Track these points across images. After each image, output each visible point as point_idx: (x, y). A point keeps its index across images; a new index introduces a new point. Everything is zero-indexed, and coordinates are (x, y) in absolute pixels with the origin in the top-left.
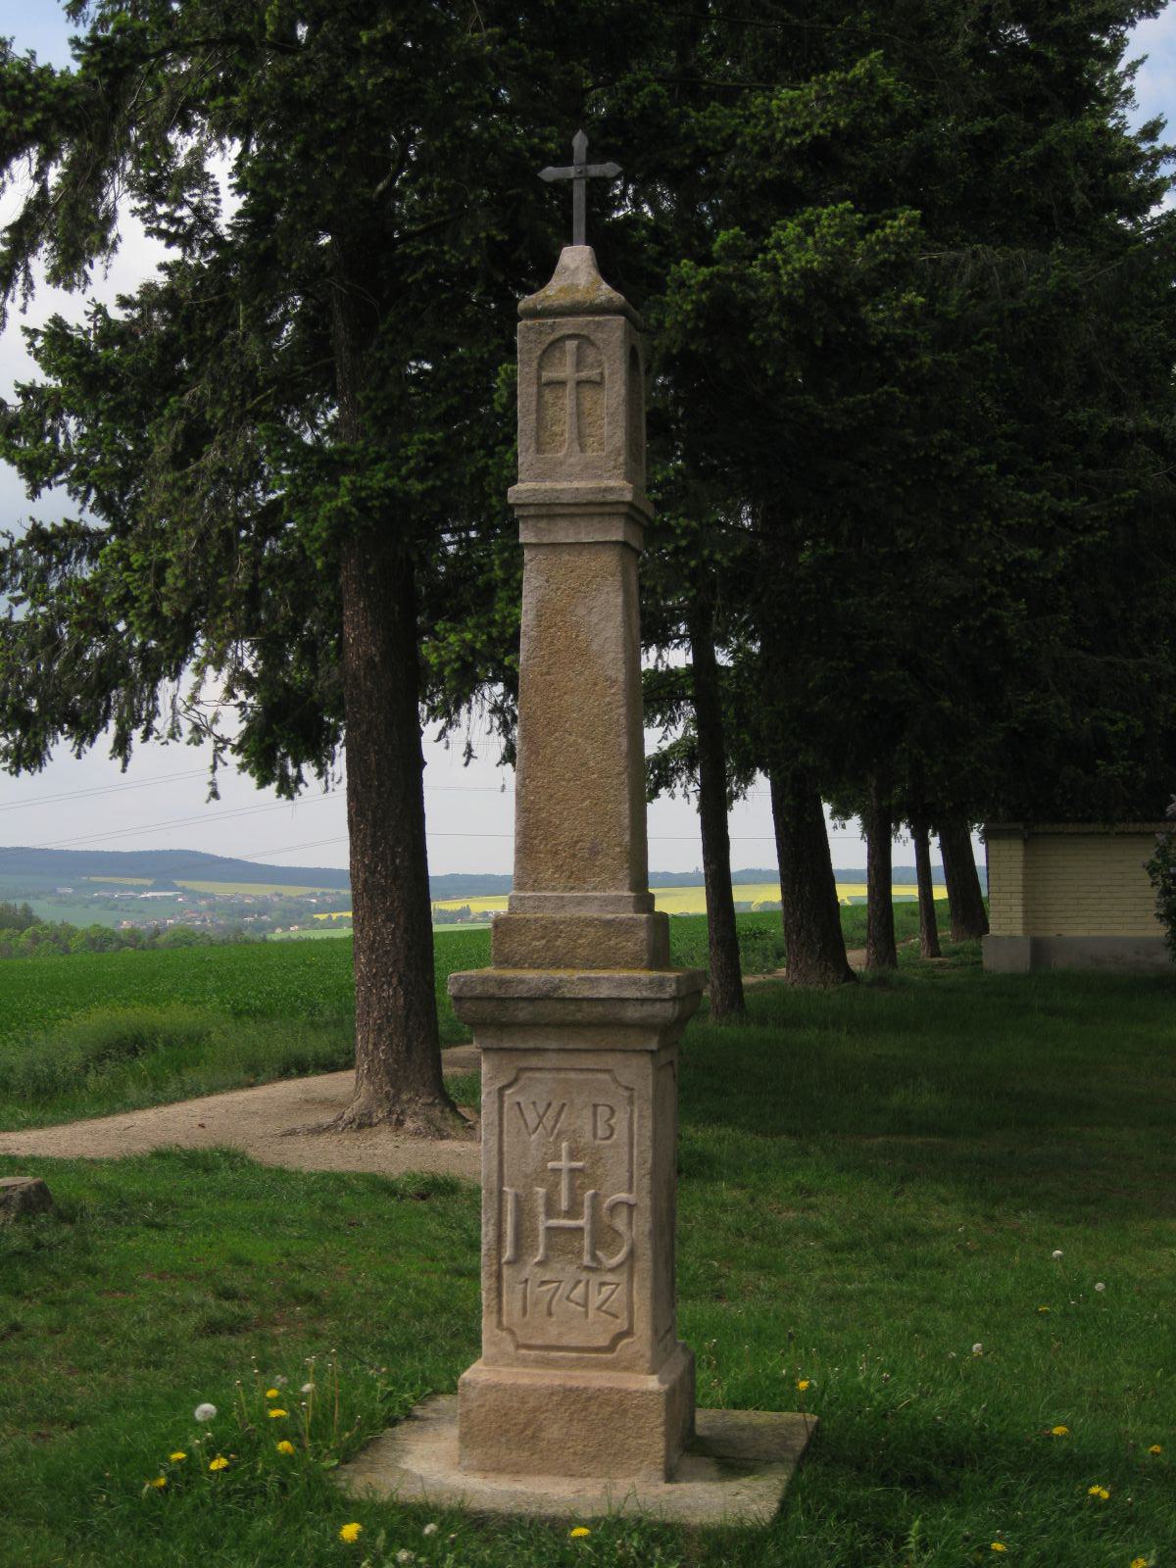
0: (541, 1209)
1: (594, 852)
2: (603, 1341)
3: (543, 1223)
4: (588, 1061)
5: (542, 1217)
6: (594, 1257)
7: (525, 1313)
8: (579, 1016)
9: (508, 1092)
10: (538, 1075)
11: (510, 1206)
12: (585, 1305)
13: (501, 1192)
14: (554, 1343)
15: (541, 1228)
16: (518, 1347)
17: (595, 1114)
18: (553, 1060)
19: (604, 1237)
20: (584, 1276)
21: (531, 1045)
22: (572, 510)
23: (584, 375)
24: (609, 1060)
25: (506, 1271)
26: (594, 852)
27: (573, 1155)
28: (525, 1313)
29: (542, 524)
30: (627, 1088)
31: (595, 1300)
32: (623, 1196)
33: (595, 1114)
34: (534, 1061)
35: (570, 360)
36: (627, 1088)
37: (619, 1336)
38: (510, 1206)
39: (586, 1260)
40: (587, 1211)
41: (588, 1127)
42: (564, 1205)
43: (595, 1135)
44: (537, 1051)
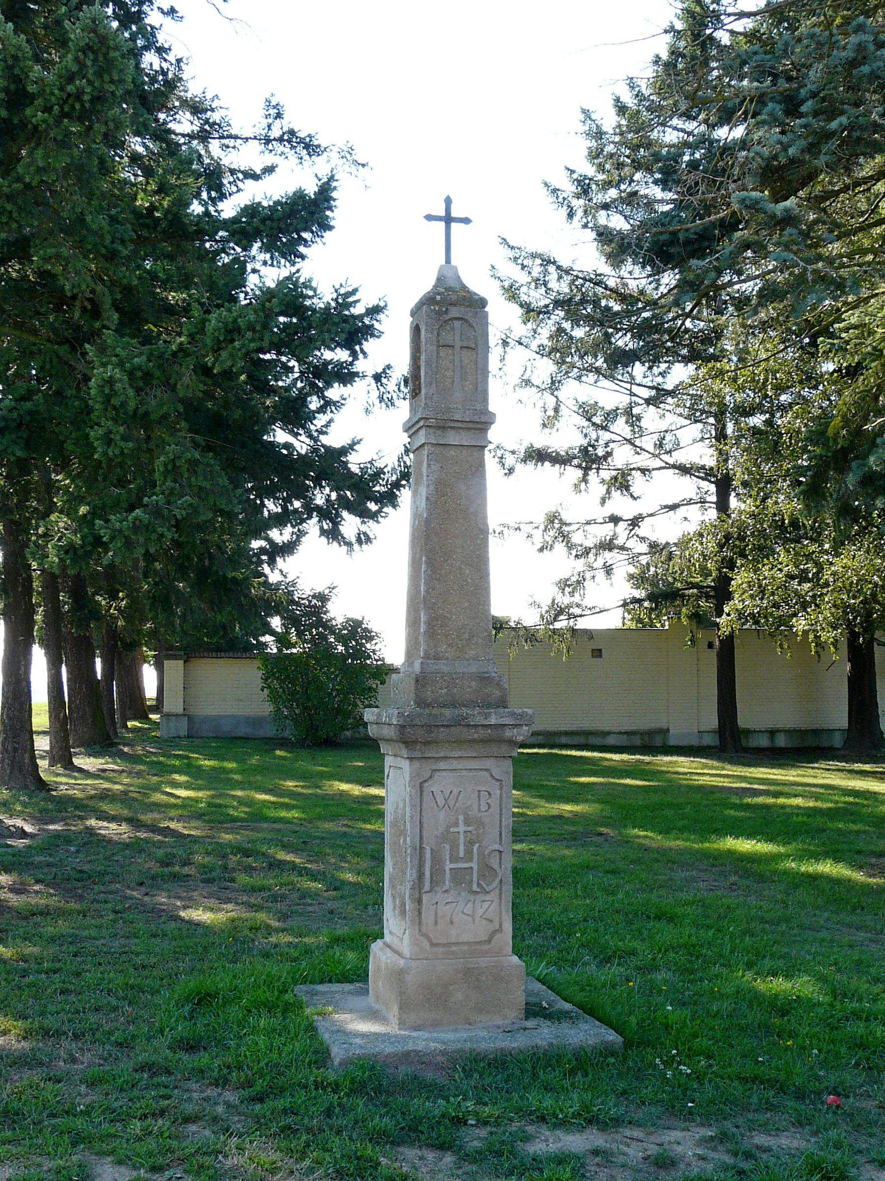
0: (448, 857)
1: (472, 637)
2: (484, 937)
3: (448, 866)
4: (475, 764)
5: (448, 862)
6: (479, 884)
7: (436, 923)
8: (476, 736)
9: (426, 784)
10: (444, 773)
11: (428, 855)
12: (473, 916)
13: (421, 848)
14: (454, 941)
15: (447, 869)
16: (432, 945)
17: (479, 796)
18: (455, 764)
19: (487, 871)
20: (472, 897)
21: (442, 754)
22: (459, 425)
23: (465, 344)
24: (489, 763)
25: (425, 897)
26: (472, 637)
27: (467, 823)
28: (436, 923)
29: (439, 432)
30: (497, 780)
31: (480, 912)
32: (497, 847)
33: (479, 796)
34: (442, 765)
35: (457, 333)
36: (497, 780)
37: (495, 932)
38: (428, 855)
39: (475, 887)
40: (475, 857)
41: (475, 806)
42: (462, 854)
43: (479, 810)
44: (446, 758)
